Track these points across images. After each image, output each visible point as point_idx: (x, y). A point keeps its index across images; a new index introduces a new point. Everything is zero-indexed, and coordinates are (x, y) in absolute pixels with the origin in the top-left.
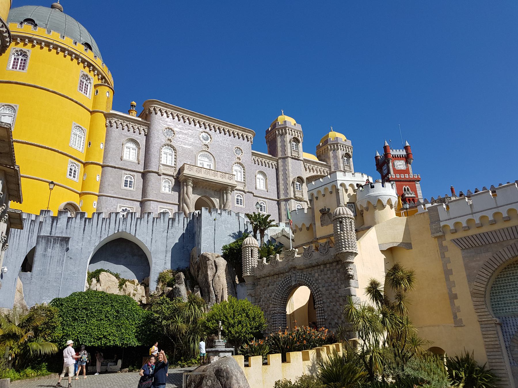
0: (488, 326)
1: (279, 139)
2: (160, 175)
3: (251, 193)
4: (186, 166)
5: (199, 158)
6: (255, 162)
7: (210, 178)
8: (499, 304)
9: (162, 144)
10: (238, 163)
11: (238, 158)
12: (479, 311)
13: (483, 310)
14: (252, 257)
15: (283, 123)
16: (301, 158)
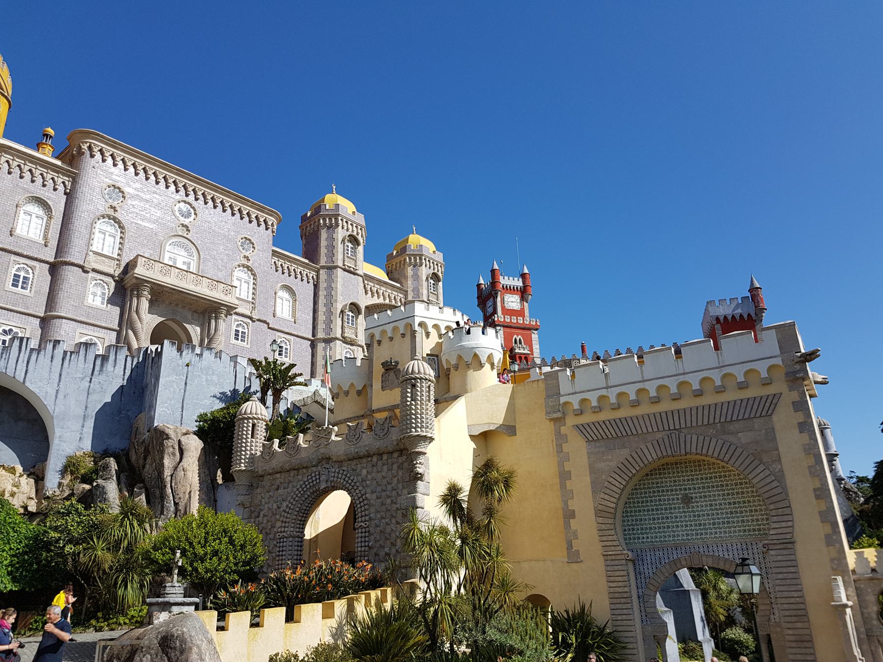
0: (616, 562)
1: (324, 234)
2: (86, 272)
3: (265, 322)
4: (141, 261)
5: (168, 248)
6: (277, 267)
7: (186, 286)
8: (633, 529)
9: (98, 214)
10: (243, 266)
11: (245, 257)
12: (604, 538)
13: (610, 538)
14: (252, 437)
15: (333, 207)
16: (359, 272)
